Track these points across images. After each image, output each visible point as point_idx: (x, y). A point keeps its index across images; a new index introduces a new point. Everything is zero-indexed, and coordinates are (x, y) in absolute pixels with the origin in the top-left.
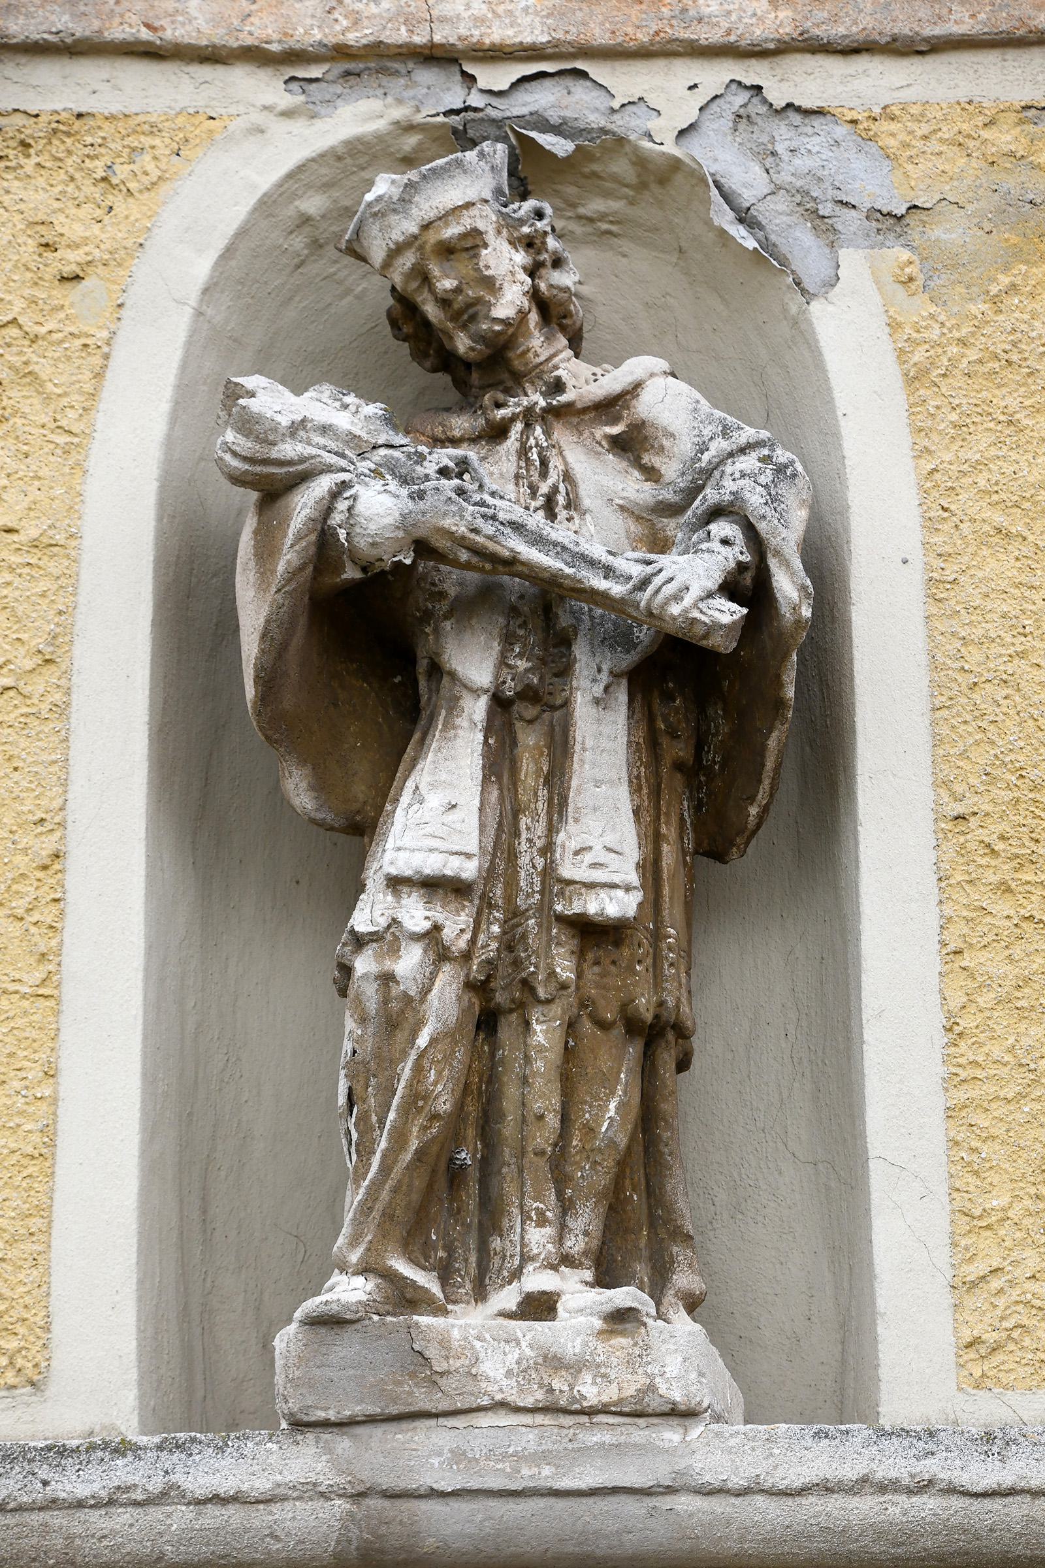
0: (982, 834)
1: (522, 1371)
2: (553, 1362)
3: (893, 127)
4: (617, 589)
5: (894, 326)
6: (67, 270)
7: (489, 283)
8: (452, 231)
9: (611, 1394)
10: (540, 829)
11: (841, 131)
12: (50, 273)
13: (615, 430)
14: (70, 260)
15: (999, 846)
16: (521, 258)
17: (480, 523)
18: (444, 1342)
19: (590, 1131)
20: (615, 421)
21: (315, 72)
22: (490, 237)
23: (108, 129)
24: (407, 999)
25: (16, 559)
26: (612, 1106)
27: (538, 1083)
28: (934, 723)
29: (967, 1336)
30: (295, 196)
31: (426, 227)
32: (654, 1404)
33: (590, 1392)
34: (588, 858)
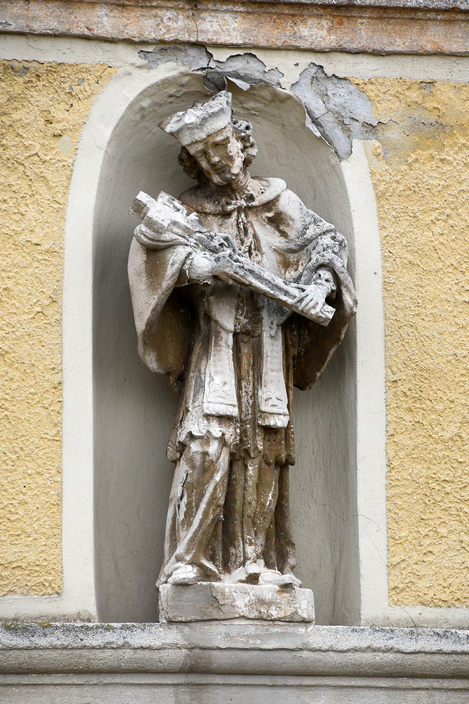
1: (250, 605)
2: (261, 602)
3: (372, 87)
5: (372, 173)
8: (219, 138)
9: (282, 614)
10: (250, 388)
11: (352, 88)
12: (50, 133)
13: (270, 215)
14: (57, 127)
15: (408, 393)
20: (270, 210)
21: (150, 49)
24: (212, 462)
25: (40, 257)
26: (270, 495)
27: (250, 490)
29: (392, 585)
32: (296, 618)
33: (274, 613)
34: (270, 402)
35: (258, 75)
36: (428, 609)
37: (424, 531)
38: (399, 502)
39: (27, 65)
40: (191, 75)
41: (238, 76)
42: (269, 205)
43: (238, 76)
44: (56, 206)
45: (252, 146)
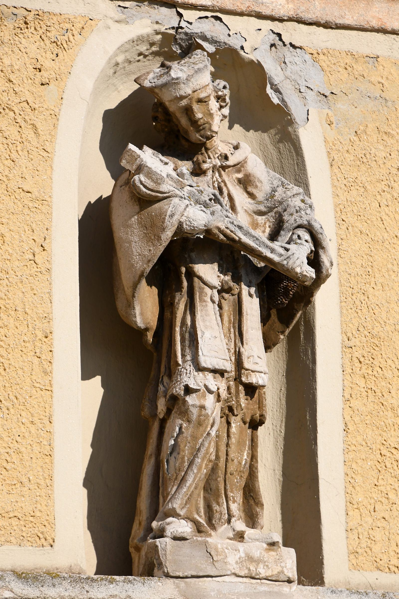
1: (240, 562)
9: (269, 573)
11: (308, 57)
12: (38, 81)
13: (240, 176)
15: (362, 359)
20: (239, 171)
26: (245, 454)
28: (341, 307)
33: (263, 572)
35: (223, 38)
36: (384, 574)
44: (45, 154)
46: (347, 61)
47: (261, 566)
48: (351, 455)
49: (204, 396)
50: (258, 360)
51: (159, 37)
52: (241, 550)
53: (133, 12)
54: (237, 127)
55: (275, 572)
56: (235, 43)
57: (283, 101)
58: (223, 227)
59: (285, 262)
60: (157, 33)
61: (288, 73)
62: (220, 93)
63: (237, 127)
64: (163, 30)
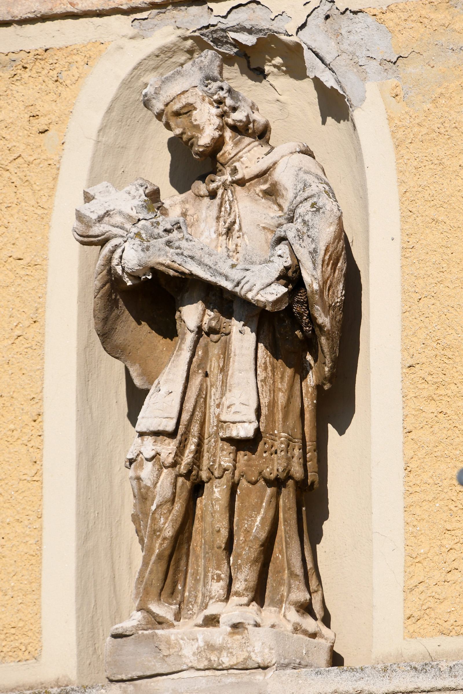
0: (422, 373)
1: (198, 653)
2: (210, 647)
3: (393, 15)
4: (229, 286)
5: (390, 119)
6: (41, 129)
7: (197, 128)
8: (176, 106)
9: (233, 661)
10: (218, 395)
11: (370, 20)
12: (35, 130)
13: (264, 187)
14: (41, 123)
15: (429, 378)
16: (215, 111)
17: (175, 258)
18: (168, 642)
19: (248, 532)
20: (265, 182)
21: (145, 15)
22: (198, 105)
23: (59, 53)
24: (148, 488)
25: (22, 272)
26: (259, 519)
27: (217, 515)
28: (403, 320)
29: (408, 614)
30: (139, 77)
31: (167, 105)
32: (250, 664)
33: (226, 660)
34: (233, 409)
35: (265, 25)
36: (449, 639)
37: (448, 543)
38: (418, 511)
39: (13, 56)
40: (191, 37)
41: (242, 29)
42: (262, 175)
43: (242, 29)
44: (40, 211)
45: (234, 109)
46: (423, 12)
47: (224, 653)
48: (415, 498)
49: (141, 466)
50: (243, 408)
51: (190, 42)
52: (200, 638)
53: (155, 21)
54: (329, 120)
55: (241, 659)
56: (275, 26)
57: (338, 82)
58: (168, 262)
59: (237, 289)
60: (186, 39)
61: (345, 46)
62: (216, 97)
63: (329, 120)
64: (188, 34)
